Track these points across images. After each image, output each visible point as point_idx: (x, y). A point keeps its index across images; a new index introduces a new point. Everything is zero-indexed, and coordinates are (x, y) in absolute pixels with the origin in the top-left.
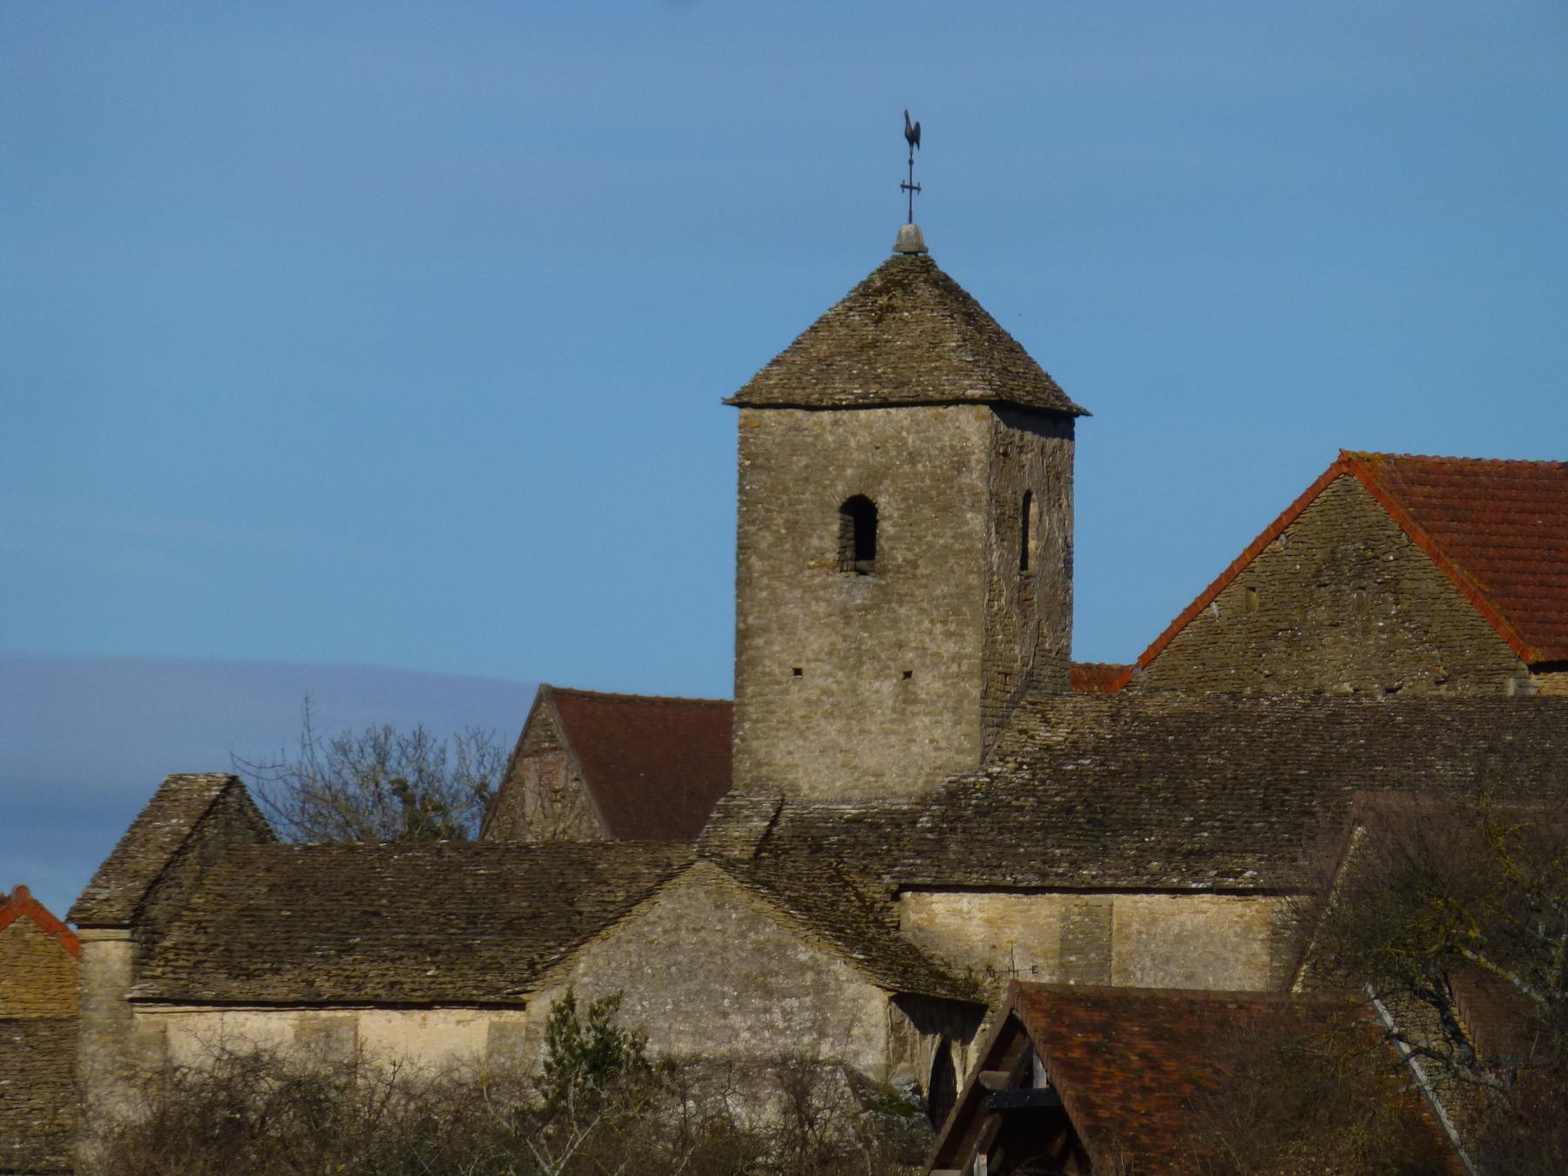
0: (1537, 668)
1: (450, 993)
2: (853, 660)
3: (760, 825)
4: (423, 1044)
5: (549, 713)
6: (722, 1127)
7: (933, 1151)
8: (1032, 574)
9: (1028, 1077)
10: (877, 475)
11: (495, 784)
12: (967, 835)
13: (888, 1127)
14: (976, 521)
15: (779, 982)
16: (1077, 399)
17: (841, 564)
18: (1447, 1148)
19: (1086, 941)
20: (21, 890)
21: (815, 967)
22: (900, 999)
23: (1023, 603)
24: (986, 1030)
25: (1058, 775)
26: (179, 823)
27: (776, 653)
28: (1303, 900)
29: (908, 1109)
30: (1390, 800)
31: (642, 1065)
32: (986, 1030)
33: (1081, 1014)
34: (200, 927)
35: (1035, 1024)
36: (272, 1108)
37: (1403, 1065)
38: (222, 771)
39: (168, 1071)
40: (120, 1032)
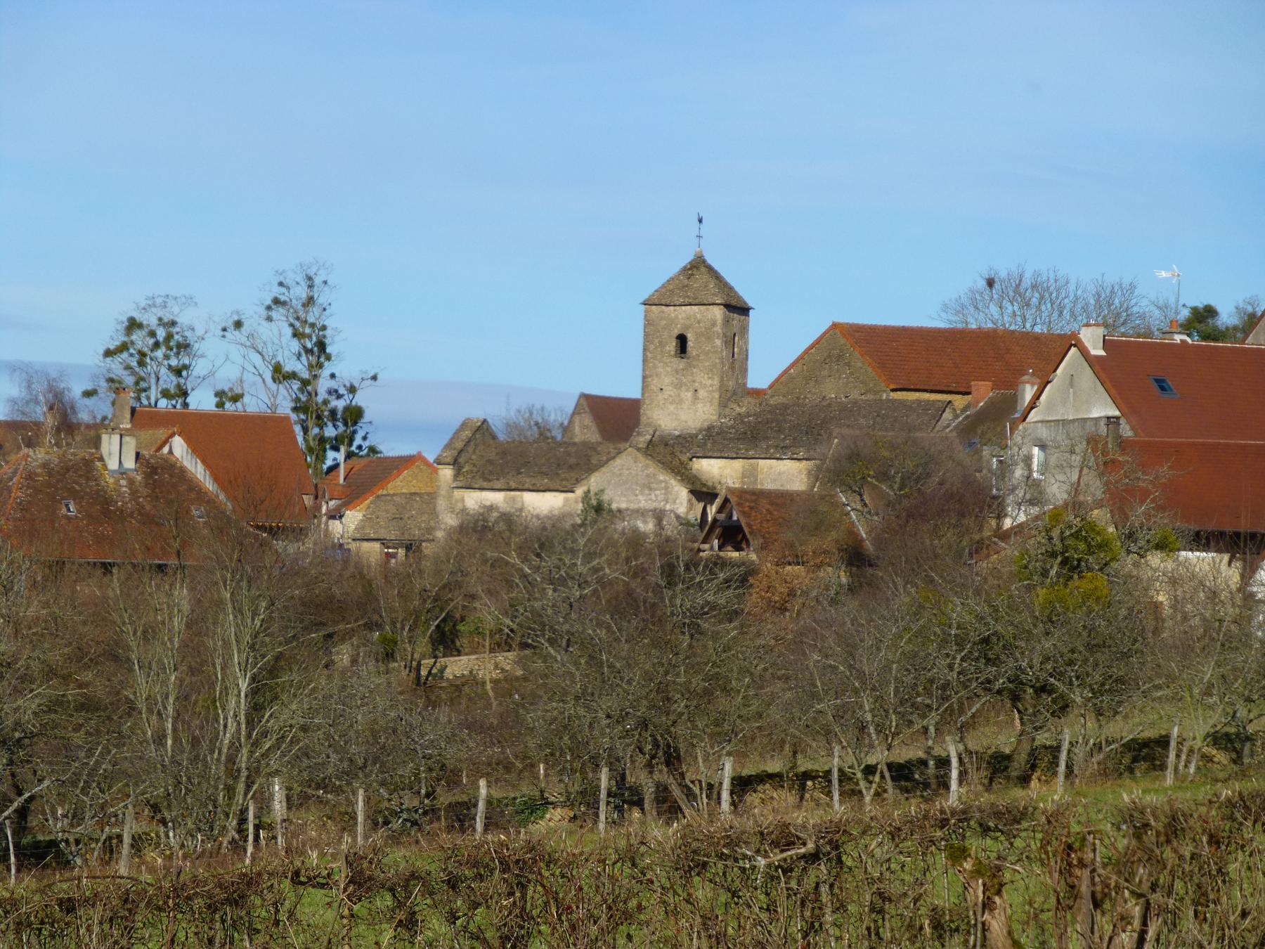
0: (893, 390)
1: (552, 487)
2: (679, 386)
3: (649, 437)
4: (543, 504)
5: (583, 401)
6: (635, 531)
7: (701, 539)
8: (736, 362)
9: (731, 516)
10: (687, 327)
11: (566, 423)
12: (714, 441)
13: (687, 531)
14: (718, 342)
15: (654, 486)
16: (750, 304)
17: (676, 355)
18: (862, 540)
19: (751, 474)
20: (419, 453)
21: (665, 481)
22: (692, 492)
23: (733, 368)
24: (718, 502)
25: (742, 423)
26: (468, 433)
27: (654, 383)
28: (818, 462)
29: (693, 526)
30: (845, 431)
31: (610, 511)
32: (718, 502)
33: (748, 497)
34: (474, 465)
35: (733, 500)
36: (496, 522)
37: (848, 514)
38: (481, 418)
39: (464, 510)
40: (450, 497)
